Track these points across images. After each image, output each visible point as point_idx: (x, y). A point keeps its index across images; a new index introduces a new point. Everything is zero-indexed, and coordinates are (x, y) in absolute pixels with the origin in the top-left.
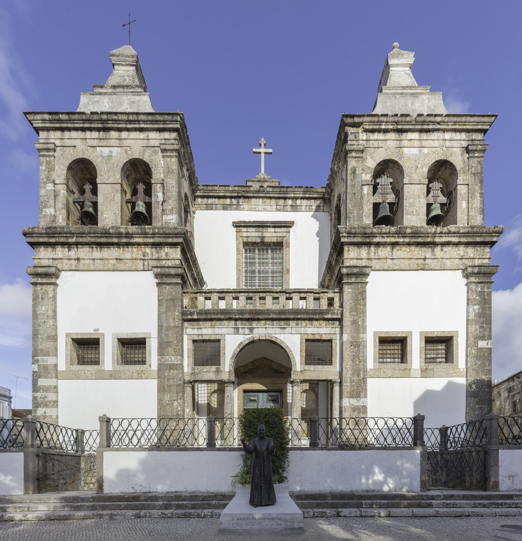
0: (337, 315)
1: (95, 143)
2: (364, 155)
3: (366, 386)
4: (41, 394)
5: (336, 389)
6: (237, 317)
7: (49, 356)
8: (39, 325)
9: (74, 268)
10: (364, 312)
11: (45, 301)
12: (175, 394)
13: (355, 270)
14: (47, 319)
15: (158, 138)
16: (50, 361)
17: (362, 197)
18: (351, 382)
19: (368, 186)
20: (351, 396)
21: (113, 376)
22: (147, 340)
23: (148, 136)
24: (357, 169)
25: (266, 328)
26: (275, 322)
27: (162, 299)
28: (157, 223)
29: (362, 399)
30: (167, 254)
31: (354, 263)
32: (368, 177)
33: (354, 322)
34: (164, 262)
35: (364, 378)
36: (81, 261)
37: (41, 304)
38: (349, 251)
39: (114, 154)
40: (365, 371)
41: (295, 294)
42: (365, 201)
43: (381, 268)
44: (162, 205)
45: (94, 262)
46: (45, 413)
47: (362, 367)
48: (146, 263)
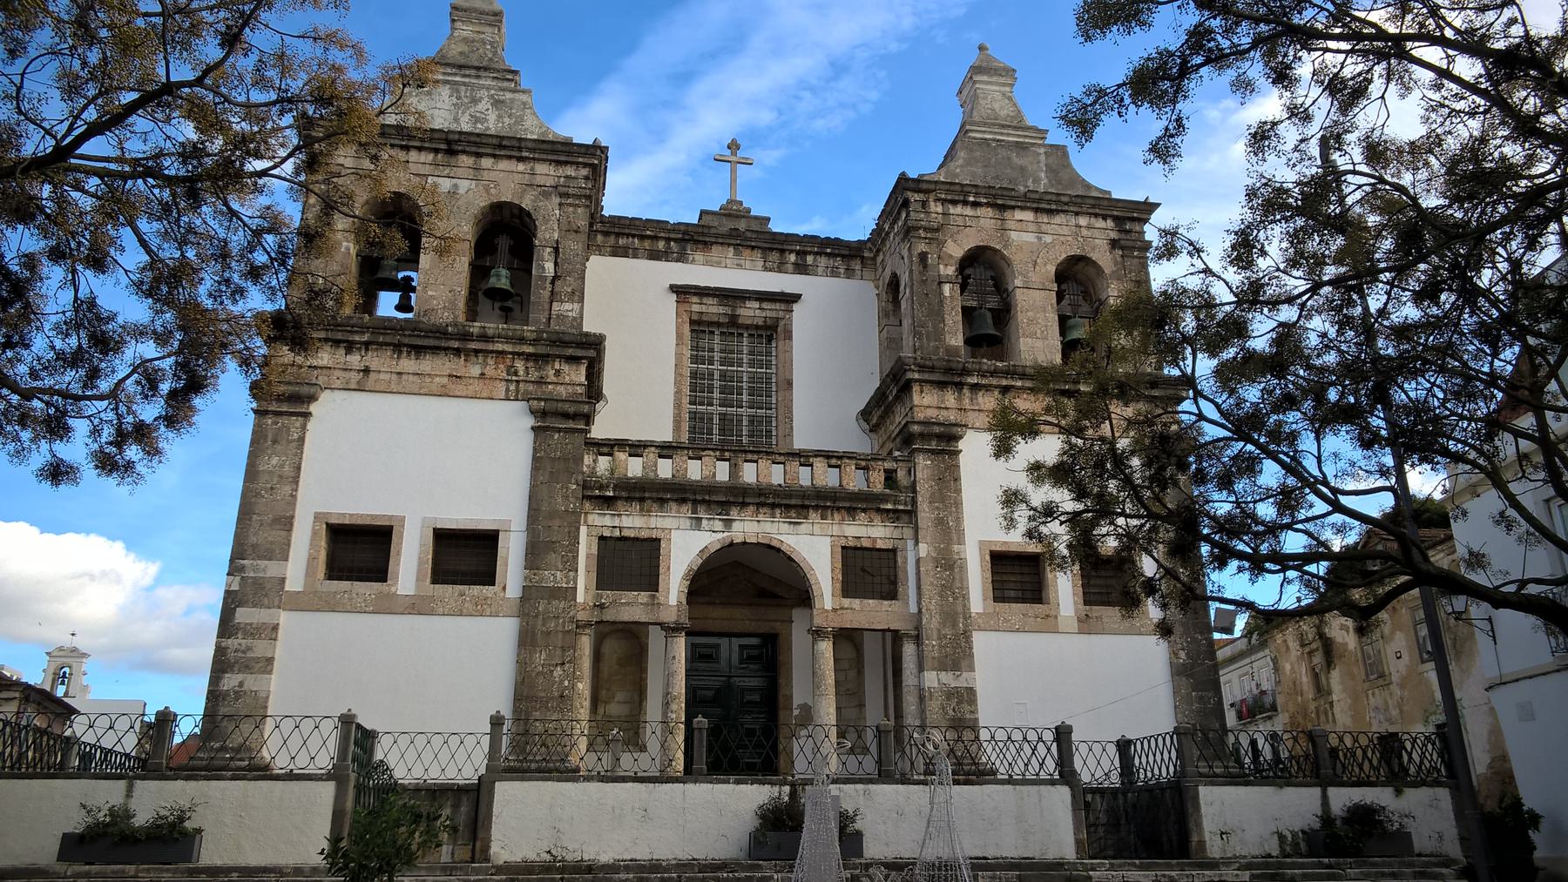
0: (905, 504)
1: (426, 170)
2: (940, 236)
3: (971, 648)
4: (239, 641)
5: (909, 649)
6: (699, 497)
7: (270, 559)
8: (258, 494)
9: (353, 387)
10: (958, 504)
11: (278, 447)
12: (559, 652)
13: (937, 429)
14: (278, 483)
15: (552, 173)
16: (271, 569)
17: (941, 301)
18: (939, 638)
20: (942, 667)
21: (416, 606)
22: (501, 535)
23: (532, 169)
25: (759, 521)
26: (778, 512)
27: (541, 457)
28: (538, 316)
29: (965, 674)
30: (558, 373)
31: (931, 413)
32: (950, 271)
33: (940, 522)
34: (550, 387)
35: (965, 632)
36: (372, 376)
37: (269, 452)
38: (922, 392)
39: (462, 191)
40: (967, 616)
41: (818, 459)
42: (947, 308)
44: (553, 283)
45: (400, 378)
46: (241, 684)
47: (960, 609)
48: (512, 387)
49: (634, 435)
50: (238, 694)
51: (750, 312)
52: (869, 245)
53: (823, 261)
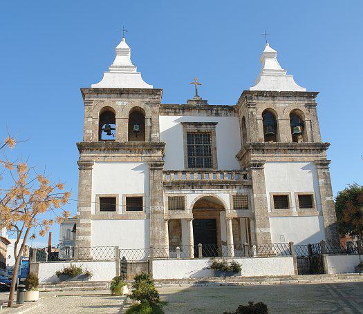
5: (252, 222)
21: (123, 218)
49: (175, 169)
50: (83, 241)
51: (203, 129)
53: (223, 112)
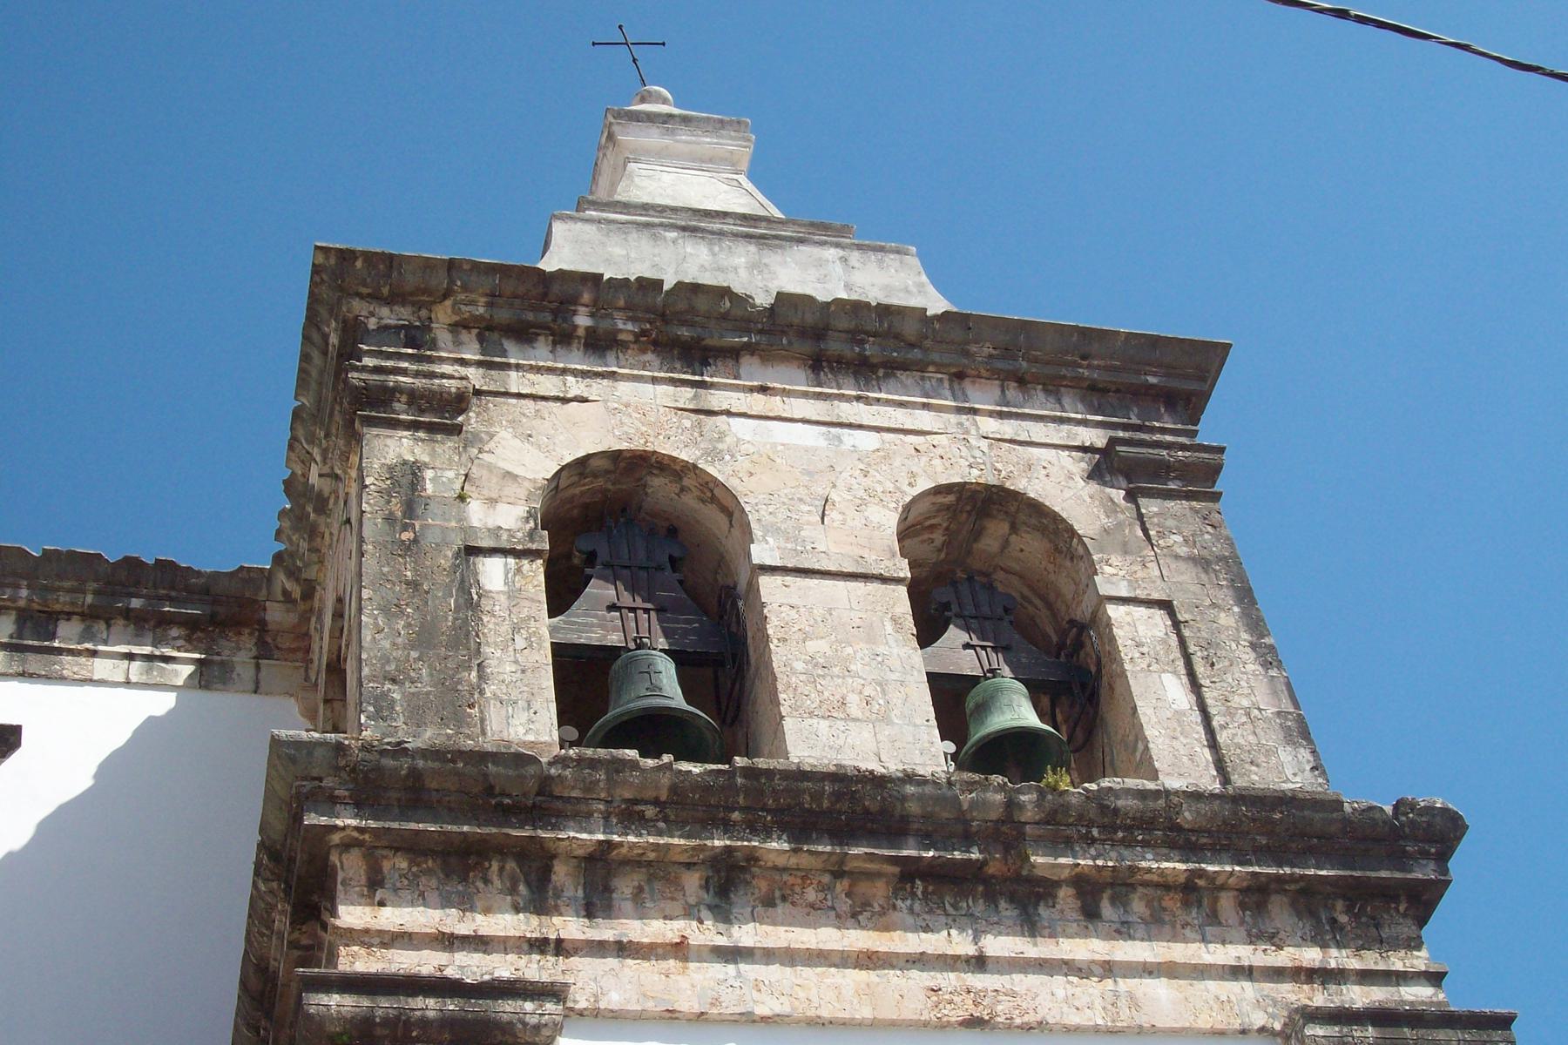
19: (511, 561)
24: (429, 474)
42: (494, 628)
43: (650, 1005)
52: (281, 578)
